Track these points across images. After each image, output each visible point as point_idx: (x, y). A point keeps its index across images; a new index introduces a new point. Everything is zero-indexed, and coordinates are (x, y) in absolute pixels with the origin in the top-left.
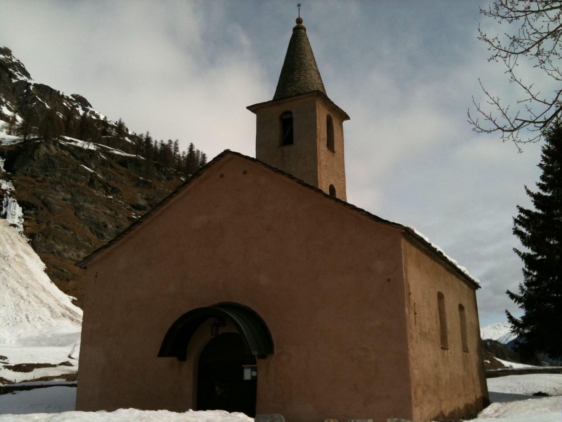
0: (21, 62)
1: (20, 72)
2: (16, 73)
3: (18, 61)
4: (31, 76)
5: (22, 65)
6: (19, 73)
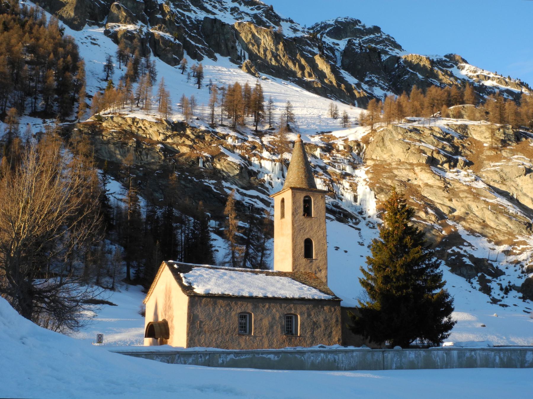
0: (391, 36)
1: (392, 46)
2: (387, 49)
3: (388, 35)
4: (403, 48)
5: (392, 39)
6: (390, 47)
